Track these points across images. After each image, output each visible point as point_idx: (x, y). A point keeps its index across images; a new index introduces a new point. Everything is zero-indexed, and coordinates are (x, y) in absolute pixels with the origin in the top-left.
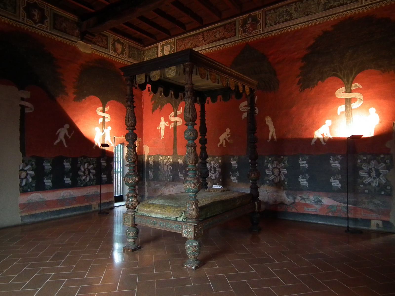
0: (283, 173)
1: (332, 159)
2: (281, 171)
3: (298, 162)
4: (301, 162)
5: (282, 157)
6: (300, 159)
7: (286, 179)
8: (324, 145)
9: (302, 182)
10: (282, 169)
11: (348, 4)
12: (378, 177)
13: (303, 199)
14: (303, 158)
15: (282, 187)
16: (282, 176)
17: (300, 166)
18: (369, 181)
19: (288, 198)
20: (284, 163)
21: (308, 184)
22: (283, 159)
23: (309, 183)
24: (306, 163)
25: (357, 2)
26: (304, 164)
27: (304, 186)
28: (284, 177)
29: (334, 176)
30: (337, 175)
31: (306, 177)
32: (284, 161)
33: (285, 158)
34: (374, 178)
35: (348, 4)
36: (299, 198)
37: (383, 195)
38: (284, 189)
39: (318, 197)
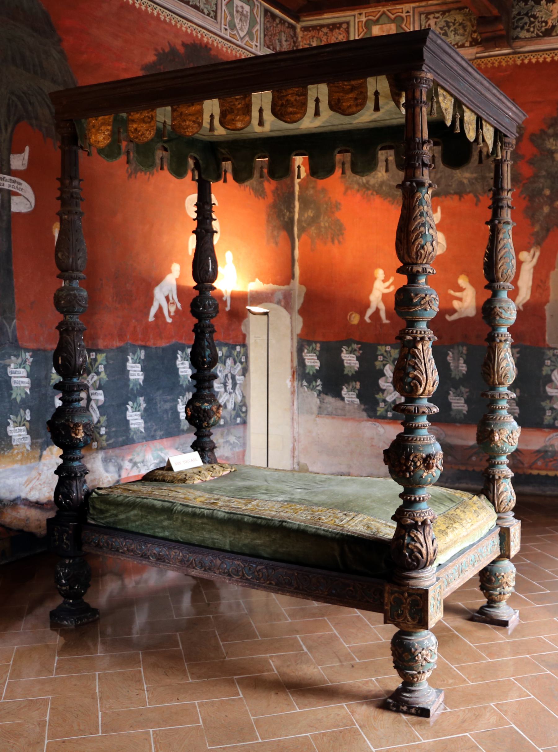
0: (97, 401)
1: (180, 358)
2: (93, 397)
3: (125, 366)
4: (132, 367)
5: (94, 353)
6: (130, 358)
7: (104, 419)
8: (168, 323)
9: (132, 420)
10: (95, 391)
11: (204, 13)
12: (234, 391)
13: (135, 464)
14: (136, 357)
15: (95, 444)
16: (94, 410)
17: (128, 379)
18: (224, 401)
19: (107, 471)
20: (98, 373)
21: (143, 425)
22: (95, 360)
23: (145, 422)
24: (140, 369)
25: (215, 21)
26: (136, 373)
27: (137, 431)
28: (98, 415)
29: (183, 396)
30: (187, 393)
31: (140, 405)
32: (98, 367)
33: (101, 357)
34: (230, 393)
35: (204, 13)
36: (127, 465)
37: (238, 424)
38: (101, 448)
39: (160, 453)
